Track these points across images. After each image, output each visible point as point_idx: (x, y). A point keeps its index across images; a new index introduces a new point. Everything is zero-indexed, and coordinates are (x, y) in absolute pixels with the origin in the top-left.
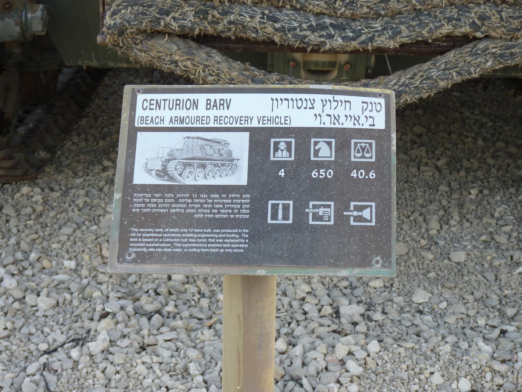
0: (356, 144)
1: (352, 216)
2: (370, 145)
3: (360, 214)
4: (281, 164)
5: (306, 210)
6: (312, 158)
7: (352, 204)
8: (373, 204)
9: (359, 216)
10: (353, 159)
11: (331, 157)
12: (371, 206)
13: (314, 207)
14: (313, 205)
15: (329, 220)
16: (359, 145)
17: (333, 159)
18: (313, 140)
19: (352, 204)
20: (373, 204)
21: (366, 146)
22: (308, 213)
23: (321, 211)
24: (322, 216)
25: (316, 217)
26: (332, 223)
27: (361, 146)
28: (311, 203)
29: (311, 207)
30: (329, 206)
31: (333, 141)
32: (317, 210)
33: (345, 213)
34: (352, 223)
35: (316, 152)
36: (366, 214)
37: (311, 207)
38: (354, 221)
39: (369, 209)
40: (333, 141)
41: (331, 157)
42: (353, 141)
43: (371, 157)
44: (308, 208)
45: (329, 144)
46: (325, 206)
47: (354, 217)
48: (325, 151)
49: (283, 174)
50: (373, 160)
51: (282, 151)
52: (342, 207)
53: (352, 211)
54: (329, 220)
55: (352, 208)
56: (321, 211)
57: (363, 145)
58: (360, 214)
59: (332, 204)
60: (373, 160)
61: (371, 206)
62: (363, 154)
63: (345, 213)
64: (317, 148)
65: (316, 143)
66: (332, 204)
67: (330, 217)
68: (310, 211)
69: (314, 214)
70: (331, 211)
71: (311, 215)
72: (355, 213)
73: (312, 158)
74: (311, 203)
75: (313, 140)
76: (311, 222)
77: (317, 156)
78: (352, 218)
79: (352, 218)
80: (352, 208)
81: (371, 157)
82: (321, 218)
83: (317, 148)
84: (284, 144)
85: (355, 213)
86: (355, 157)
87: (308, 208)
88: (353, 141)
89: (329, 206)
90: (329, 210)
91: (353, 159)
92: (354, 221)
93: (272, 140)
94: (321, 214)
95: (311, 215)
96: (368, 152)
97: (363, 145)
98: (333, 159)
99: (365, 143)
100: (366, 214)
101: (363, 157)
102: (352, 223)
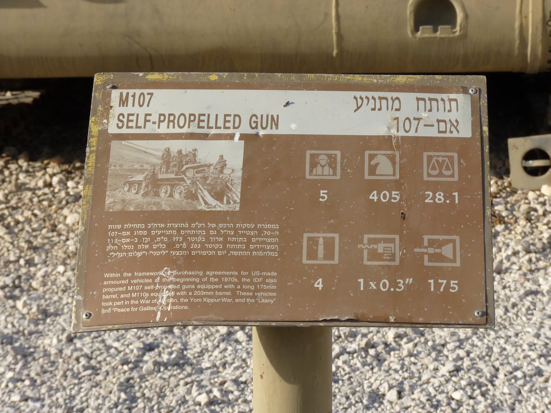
4: (326, 184)
15: (393, 259)
22: (362, 250)
24: (382, 254)
25: (374, 255)
28: (366, 237)
37: (366, 241)
46: (386, 241)
68: (365, 247)
71: (365, 252)
76: (366, 262)
94: (380, 251)
95: (365, 252)
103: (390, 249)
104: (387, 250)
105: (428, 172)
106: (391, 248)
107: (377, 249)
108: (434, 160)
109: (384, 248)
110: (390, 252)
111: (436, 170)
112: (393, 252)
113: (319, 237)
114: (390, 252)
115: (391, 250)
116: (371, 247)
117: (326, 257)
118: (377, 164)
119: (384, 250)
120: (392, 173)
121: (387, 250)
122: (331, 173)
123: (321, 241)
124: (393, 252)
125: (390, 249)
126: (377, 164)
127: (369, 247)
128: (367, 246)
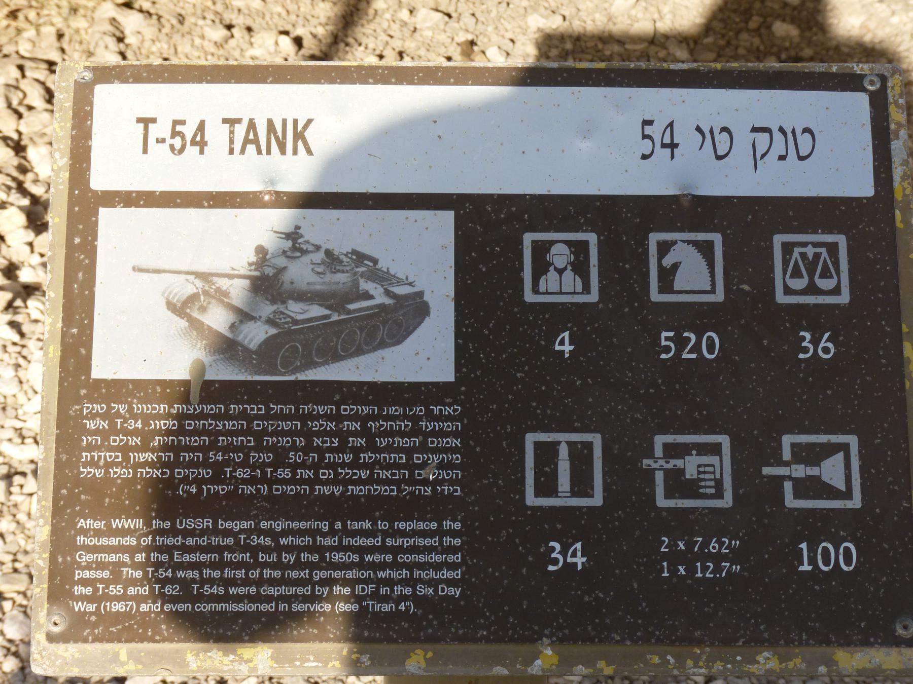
0: (788, 248)
1: (789, 478)
2: (833, 248)
3: (813, 471)
5: (646, 462)
6: (655, 296)
7: (787, 440)
8: (852, 440)
9: (808, 478)
10: (781, 298)
11: (713, 291)
12: (845, 448)
13: (672, 451)
14: (666, 446)
15: (719, 495)
16: (797, 250)
17: (719, 297)
18: (654, 238)
19: (787, 440)
20: (852, 440)
21: (817, 256)
22: (651, 473)
23: (691, 465)
25: (678, 484)
26: (727, 501)
27: (803, 256)
28: (660, 440)
29: (659, 451)
30: (715, 449)
31: (717, 238)
32: (679, 463)
33: (766, 471)
34: (790, 502)
35: (667, 276)
36: (832, 471)
37: (659, 451)
38: (797, 495)
39: (840, 456)
40: (717, 238)
41: (713, 291)
42: (778, 240)
43: (837, 291)
44: (651, 456)
45: (706, 249)
47: (797, 482)
48: (692, 271)
49: (567, 348)
50: (844, 298)
51: (560, 272)
52: (753, 453)
53: (787, 464)
54: (719, 495)
55: (787, 455)
56: (691, 465)
57: (810, 251)
58: (813, 471)
59: (724, 440)
60: (844, 298)
61: (845, 448)
62: (812, 283)
63: (766, 471)
64: (667, 261)
65: (664, 248)
66: (724, 440)
67: (719, 484)
68: (657, 465)
69: (667, 472)
70: (723, 466)
71: (659, 477)
72: (800, 471)
73: (655, 296)
74: (660, 440)
75: (654, 238)
76: (662, 502)
77: (671, 291)
78: (788, 487)
79: (788, 487)
80: (787, 455)
81: (837, 291)
82: (690, 489)
83: (667, 261)
84: (567, 251)
85: (800, 471)
86: (788, 291)
87: (651, 456)
88: (778, 240)
89: (715, 449)
90: (715, 460)
91: (781, 298)
92: (797, 495)
93: (528, 238)
95: (659, 477)
96: (825, 274)
97: (810, 251)
98: (719, 297)
99: (816, 245)
100: (832, 471)
101: (812, 289)
102: (790, 502)
103: (711, 469)
104: (705, 473)
105: (786, 287)
106: (713, 466)
107: (684, 470)
108: (796, 254)
109: (699, 466)
110: (712, 476)
111: (802, 277)
112: (718, 476)
113: (559, 443)
114: (712, 476)
115: (714, 473)
116: (670, 466)
117: (574, 494)
118: (676, 266)
119: (699, 473)
120: (709, 288)
121: (705, 473)
122: (579, 289)
123: (564, 452)
124: (718, 476)
125: (711, 469)
126: (676, 266)
127: (667, 466)
128: (662, 462)
